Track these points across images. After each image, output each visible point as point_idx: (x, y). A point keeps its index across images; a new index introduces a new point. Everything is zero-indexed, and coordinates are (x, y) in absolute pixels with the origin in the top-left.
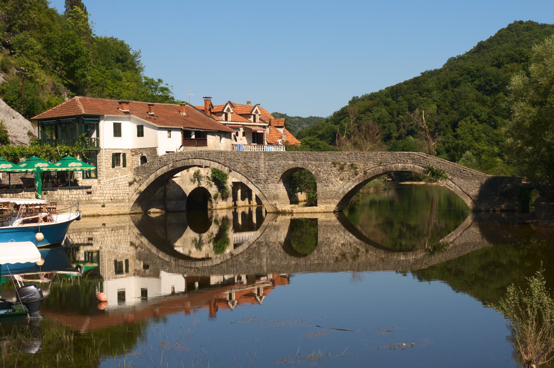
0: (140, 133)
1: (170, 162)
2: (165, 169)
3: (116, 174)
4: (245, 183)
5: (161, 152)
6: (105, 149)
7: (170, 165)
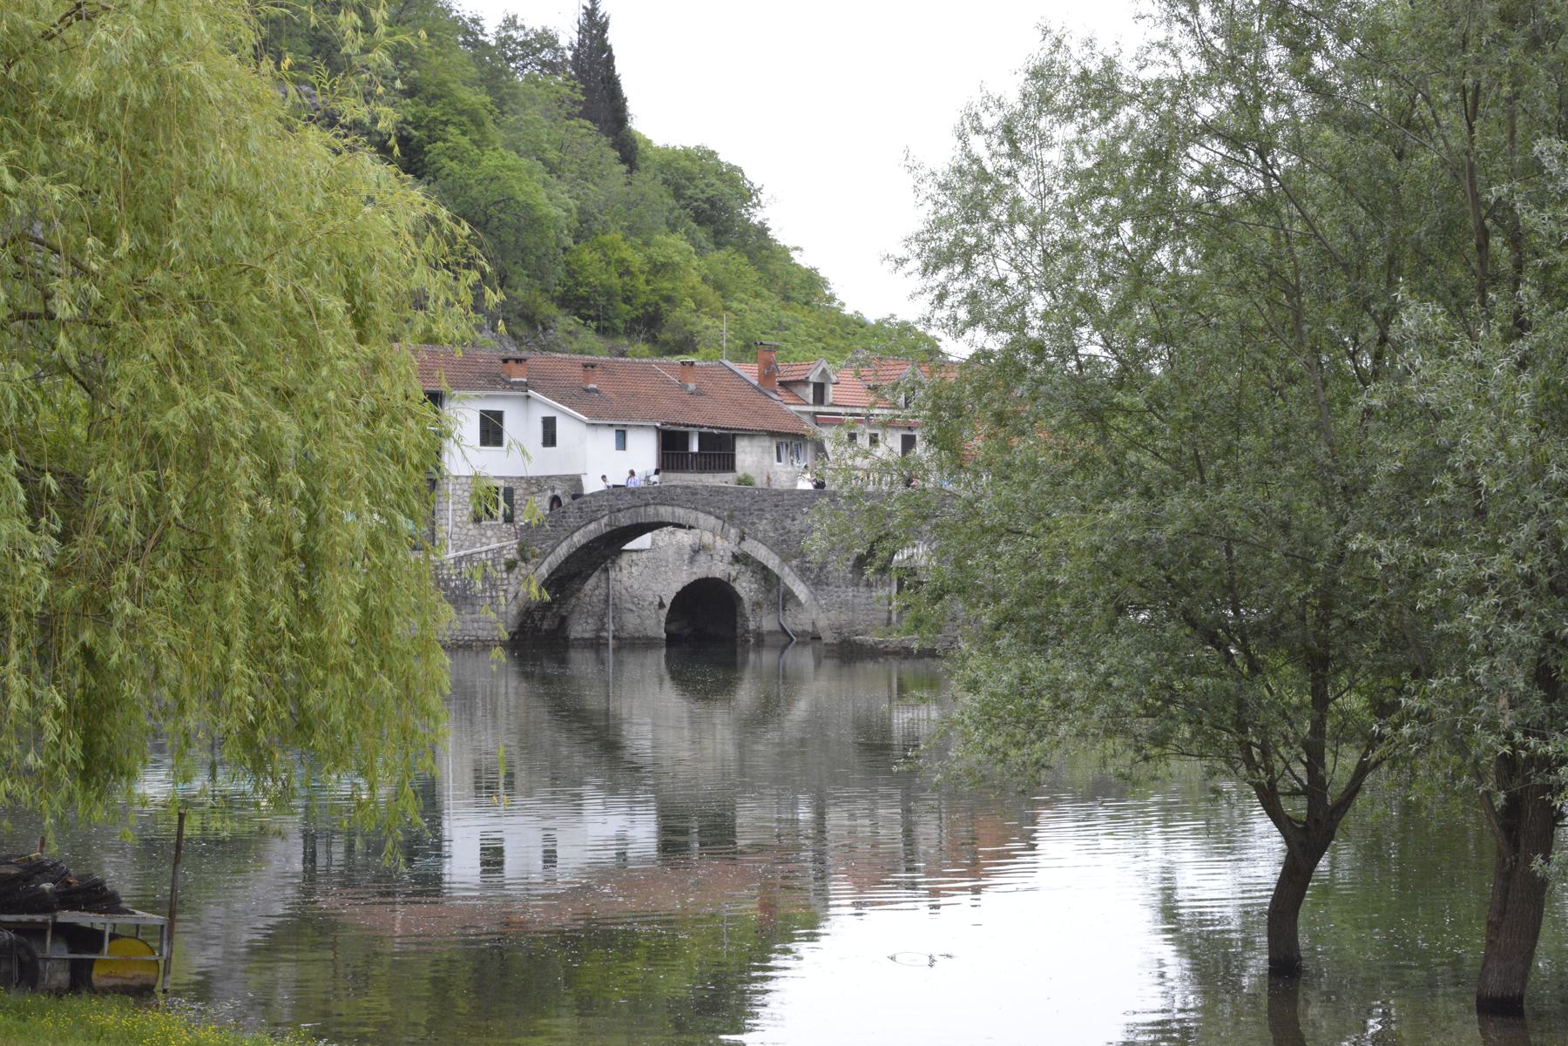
0: (549, 439)
2: (594, 529)
3: (484, 540)
5: (592, 485)
6: (457, 477)
7: (605, 520)
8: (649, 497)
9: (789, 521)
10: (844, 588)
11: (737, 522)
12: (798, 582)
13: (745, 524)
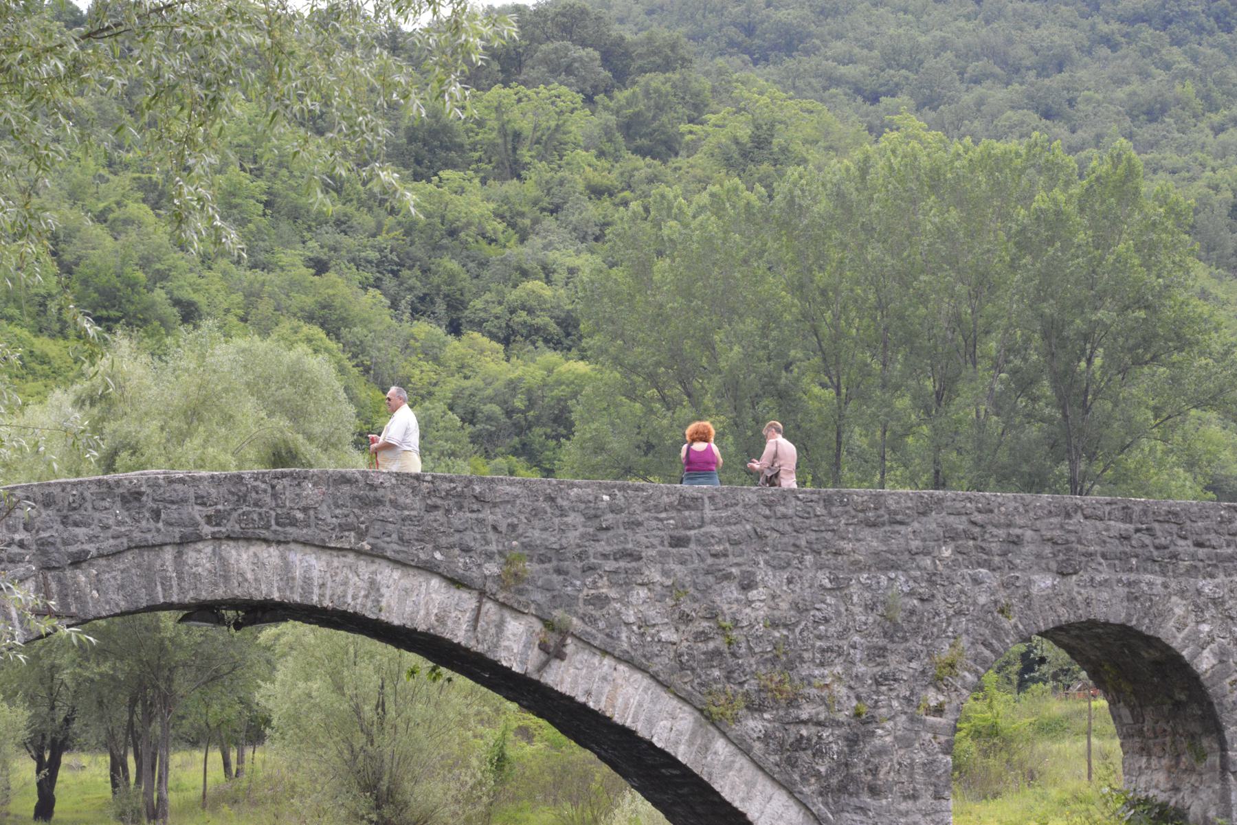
4: (683, 754)
8: (197, 512)
9: (732, 591)
10: (926, 800)
11: (538, 597)
12: (763, 785)
13: (569, 603)
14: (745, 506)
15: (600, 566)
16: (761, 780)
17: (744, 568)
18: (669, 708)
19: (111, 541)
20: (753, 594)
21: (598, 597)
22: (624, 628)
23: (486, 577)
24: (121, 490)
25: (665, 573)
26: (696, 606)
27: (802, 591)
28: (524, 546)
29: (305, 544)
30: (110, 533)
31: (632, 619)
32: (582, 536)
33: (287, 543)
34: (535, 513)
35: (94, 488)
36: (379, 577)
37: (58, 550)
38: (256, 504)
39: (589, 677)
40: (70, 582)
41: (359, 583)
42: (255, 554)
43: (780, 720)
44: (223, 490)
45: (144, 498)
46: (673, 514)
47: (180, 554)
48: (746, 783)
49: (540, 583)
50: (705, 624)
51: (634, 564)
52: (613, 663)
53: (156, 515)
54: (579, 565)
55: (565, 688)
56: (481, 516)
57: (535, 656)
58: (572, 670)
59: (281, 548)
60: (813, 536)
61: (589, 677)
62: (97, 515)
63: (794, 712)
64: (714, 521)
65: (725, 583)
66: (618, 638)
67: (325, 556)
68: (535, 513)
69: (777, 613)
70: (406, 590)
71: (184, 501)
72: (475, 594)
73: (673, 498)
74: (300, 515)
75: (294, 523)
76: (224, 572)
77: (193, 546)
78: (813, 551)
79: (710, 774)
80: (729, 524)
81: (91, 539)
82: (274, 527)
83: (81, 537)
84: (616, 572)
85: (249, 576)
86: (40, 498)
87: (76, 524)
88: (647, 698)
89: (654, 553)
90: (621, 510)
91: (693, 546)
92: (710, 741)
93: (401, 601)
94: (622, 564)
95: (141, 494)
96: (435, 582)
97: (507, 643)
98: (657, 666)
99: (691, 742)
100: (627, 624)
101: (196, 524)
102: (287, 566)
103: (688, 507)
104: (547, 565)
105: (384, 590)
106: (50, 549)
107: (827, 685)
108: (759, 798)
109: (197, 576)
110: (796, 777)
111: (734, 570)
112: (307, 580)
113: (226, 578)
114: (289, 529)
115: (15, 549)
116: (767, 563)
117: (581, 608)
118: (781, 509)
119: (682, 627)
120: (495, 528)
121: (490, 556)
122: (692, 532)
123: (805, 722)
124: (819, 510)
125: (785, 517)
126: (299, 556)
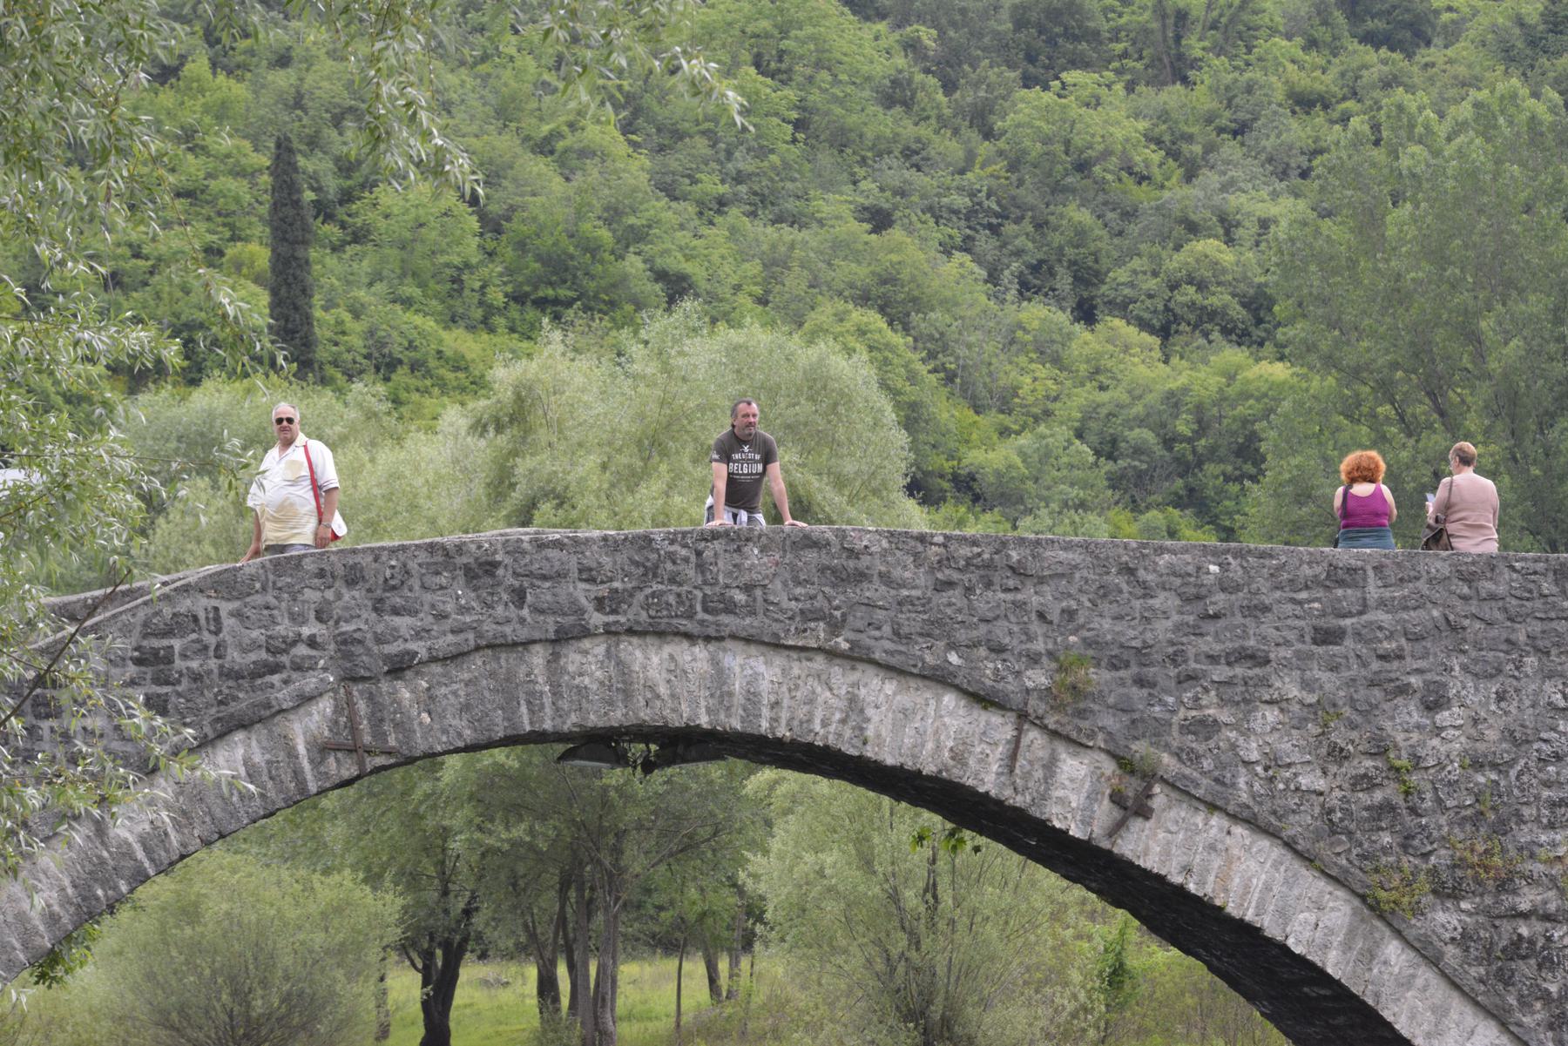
1: (310, 682)
4: (1334, 964)
8: (582, 593)
11: (1109, 721)
13: (1157, 729)
14: (1430, 581)
15: (1205, 674)
16: (1457, 1005)
17: (1428, 676)
18: (1313, 893)
19: (450, 638)
20: (1443, 717)
21: (1202, 722)
22: (1242, 770)
23: (1028, 691)
24: (465, 560)
25: (1306, 685)
26: (1354, 735)
27: (1521, 712)
28: (1088, 643)
29: (748, 640)
30: (447, 625)
31: (1255, 756)
32: (1177, 628)
33: (720, 639)
34: (1105, 592)
35: (423, 557)
36: (863, 692)
37: (369, 652)
38: (672, 581)
39: (1188, 846)
40: (387, 701)
41: (833, 701)
42: (672, 657)
43: (1487, 912)
44: (622, 558)
45: (500, 572)
46: (1320, 593)
47: (556, 657)
48: (1434, 1009)
49: (1111, 700)
50: (1369, 763)
51: (1257, 671)
52: (1225, 823)
53: (519, 596)
54: (1173, 672)
55: (1151, 863)
56: (1019, 597)
57: (1105, 812)
58: (1161, 835)
59: (711, 647)
60: (1537, 627)
61: (1188, 846)
62: (428, 597)
63: (1507, 900)
64: (1382, 604)
65: (1399, 700)
66: (1234, 785)
67: (779, 660)
68: (1105, 592)
69: (1481, 747)
70: (904, 711)
71: (560, 576)
72: (1011, 717)
73: (1318, 569)
74: (740, 597)
75: (730, 608)
76: (623, 684)
77: (575, 644)
78: (1537, 650)
79: (1377, 995)
80: (1406, 608)
81: (418, 635)
82: (701, 615)
83: (403, 631)
84: (1229, 683)
85: (663, 690)
86: (340, 571)
87: (396, 612)
88: (1280, 877)
89: (1289, 653)
90: (1238, 588)
91: (1349, 642)
92: (1377, 944)
93: (897, 728)
94: (1239, 671)
95: (495, 565)
96: (949, 699)
97: (1060, 793)
98: (1294, 827)
99: (1347, 946)
100: (1247, 763)
101: (580, 611)
102: (720, 676)
103: (1341, 583)
104: (1122, 673)
105: (870, 712)
106: (358, 649)
107: (1559, 858)
108: (1454, 1032)
109: (582, 691)
110: (1512, 1000)
111: (1413, 680)
112: (752, 697)
113: (627, 694)
114: (725, 619)
115: (302, 650)
116: (1464, 668)
117: (1175, 738)
118: (1487, 586)
119: (1333, 769)
120: (1041, 616)
121: (1034, 659)
122: (1348, 622)
123: (1524, 916)
124: (1547, 586)
125: (1492, 597)
126: (740, 660)
